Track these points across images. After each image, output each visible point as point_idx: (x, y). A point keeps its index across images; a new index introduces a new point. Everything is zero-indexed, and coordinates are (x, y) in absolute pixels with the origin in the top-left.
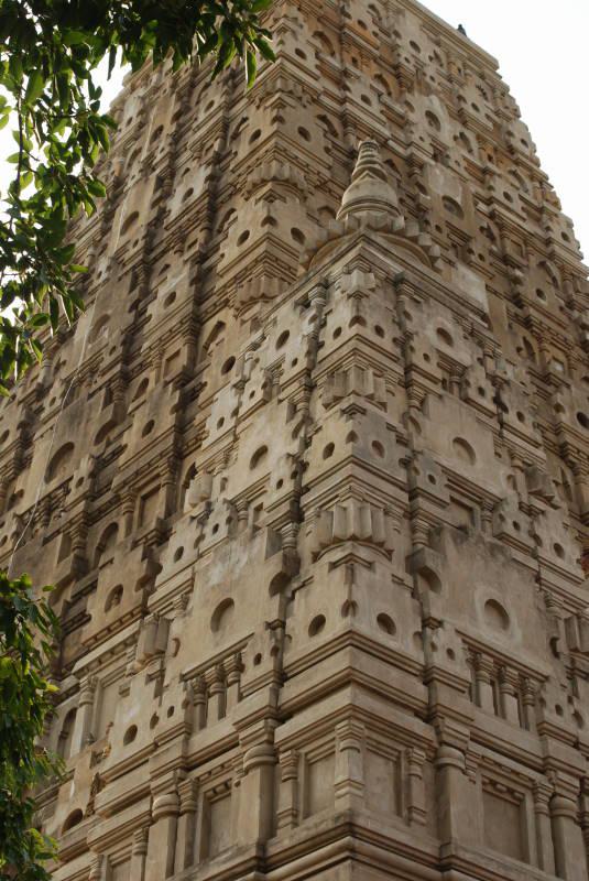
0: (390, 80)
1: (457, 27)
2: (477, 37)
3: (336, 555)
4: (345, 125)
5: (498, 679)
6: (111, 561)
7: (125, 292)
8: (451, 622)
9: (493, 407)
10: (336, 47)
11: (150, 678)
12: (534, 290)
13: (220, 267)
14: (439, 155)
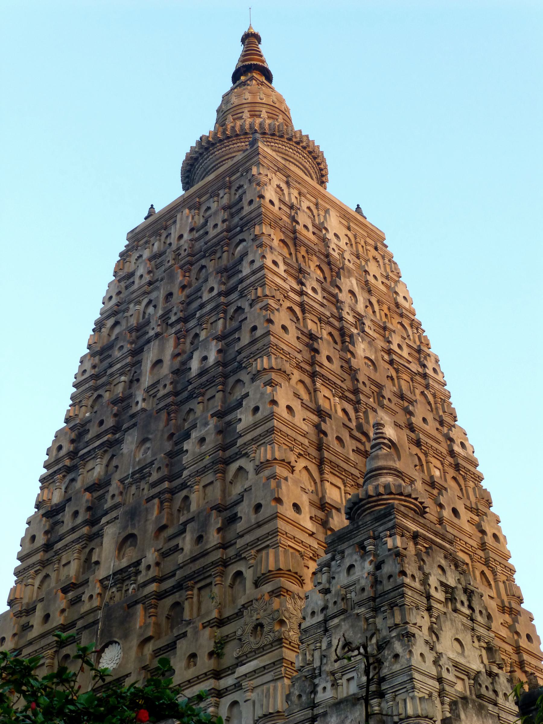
1: (354, 208)
4: (303, 311)
6: (185, 635)
12: (421, 419)
13: (240, 427)
14: (359, 319)
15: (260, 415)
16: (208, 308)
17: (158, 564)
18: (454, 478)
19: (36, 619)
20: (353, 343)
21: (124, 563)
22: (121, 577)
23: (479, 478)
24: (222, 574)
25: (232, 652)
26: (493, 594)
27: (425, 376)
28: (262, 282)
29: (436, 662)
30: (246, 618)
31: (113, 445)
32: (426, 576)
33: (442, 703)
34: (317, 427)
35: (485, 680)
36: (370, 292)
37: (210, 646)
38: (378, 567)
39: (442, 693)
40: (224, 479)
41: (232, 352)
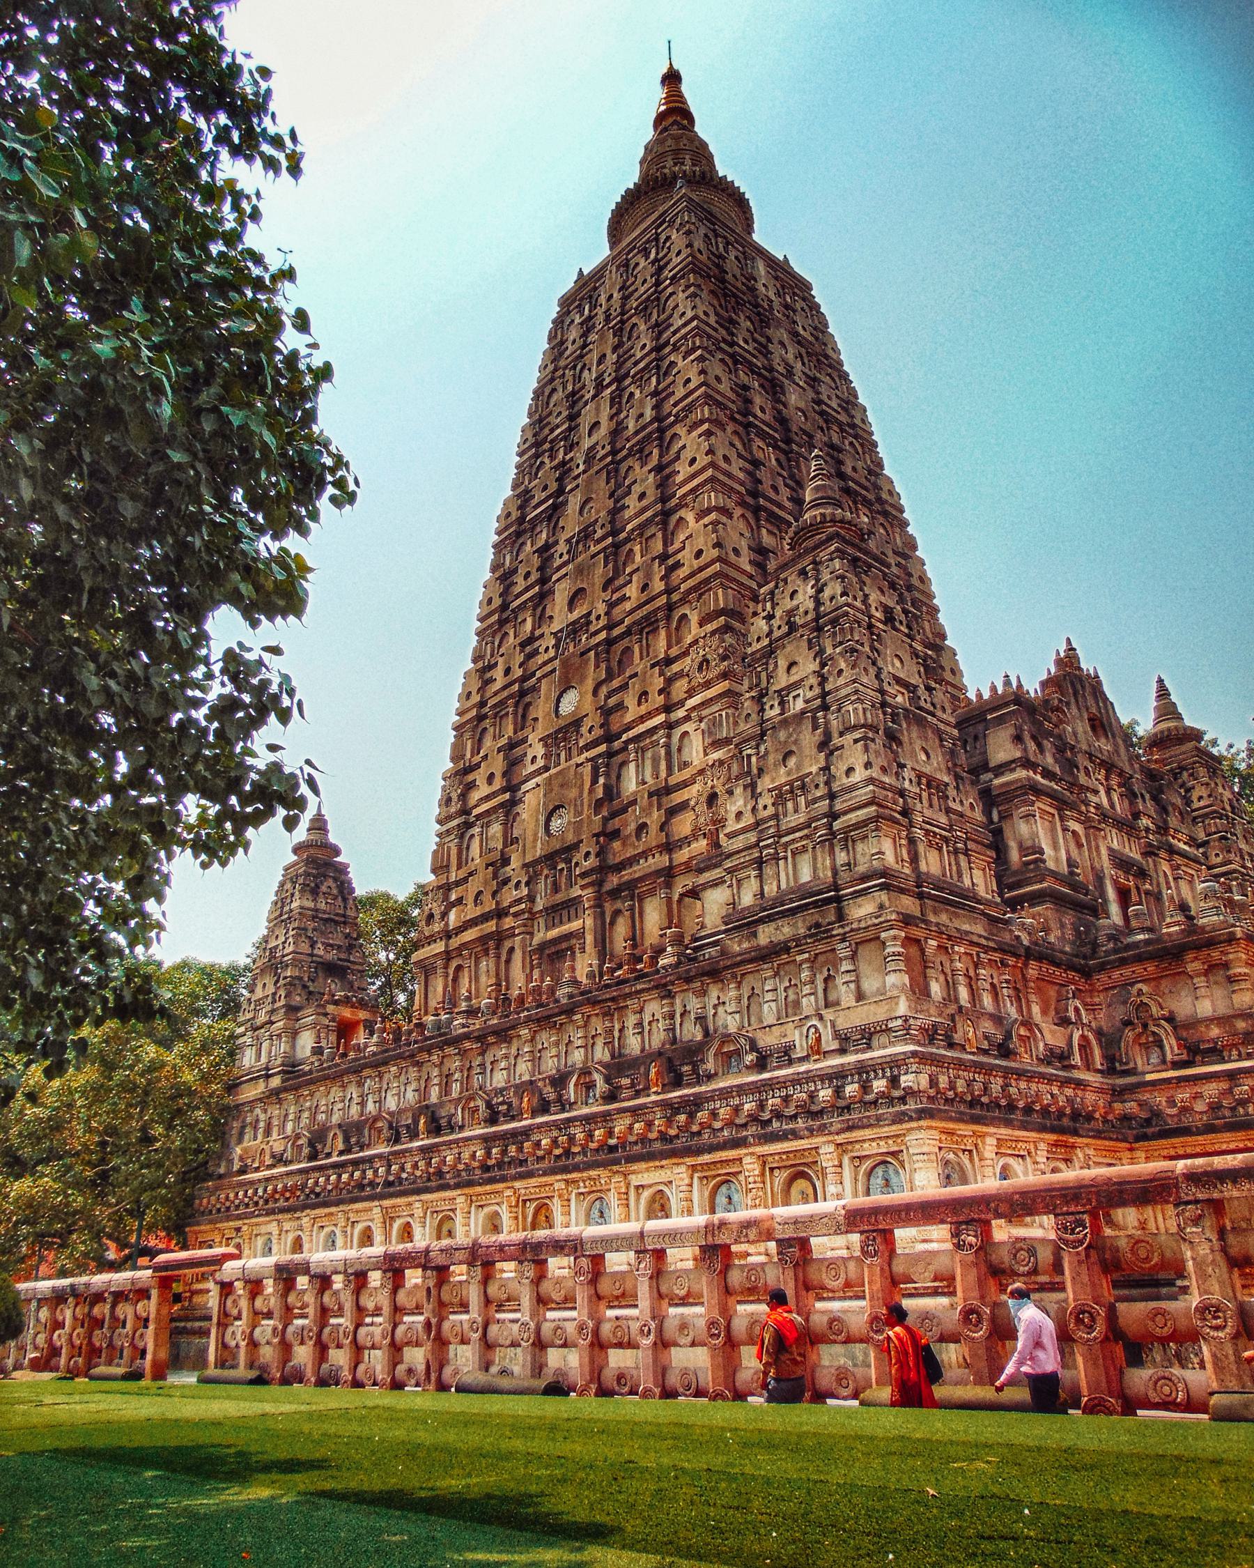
2: (799, 267)
3: (857, 735)
7: (603, 484)
8: (909, 764)
13: (679, 478)
14: (790, 374)
17: (607, 614)
19: (498, 673)
21: (576, 615)
22: (575, 629)
23: (904, 524)
24: (669, 618)
27: (853, 426)
29: (877, 676)
30: (693, 655)
32: (866, 596)
37: (659, 682)
38: (820, 590)
40: (665, 530)
41: (667, 407)
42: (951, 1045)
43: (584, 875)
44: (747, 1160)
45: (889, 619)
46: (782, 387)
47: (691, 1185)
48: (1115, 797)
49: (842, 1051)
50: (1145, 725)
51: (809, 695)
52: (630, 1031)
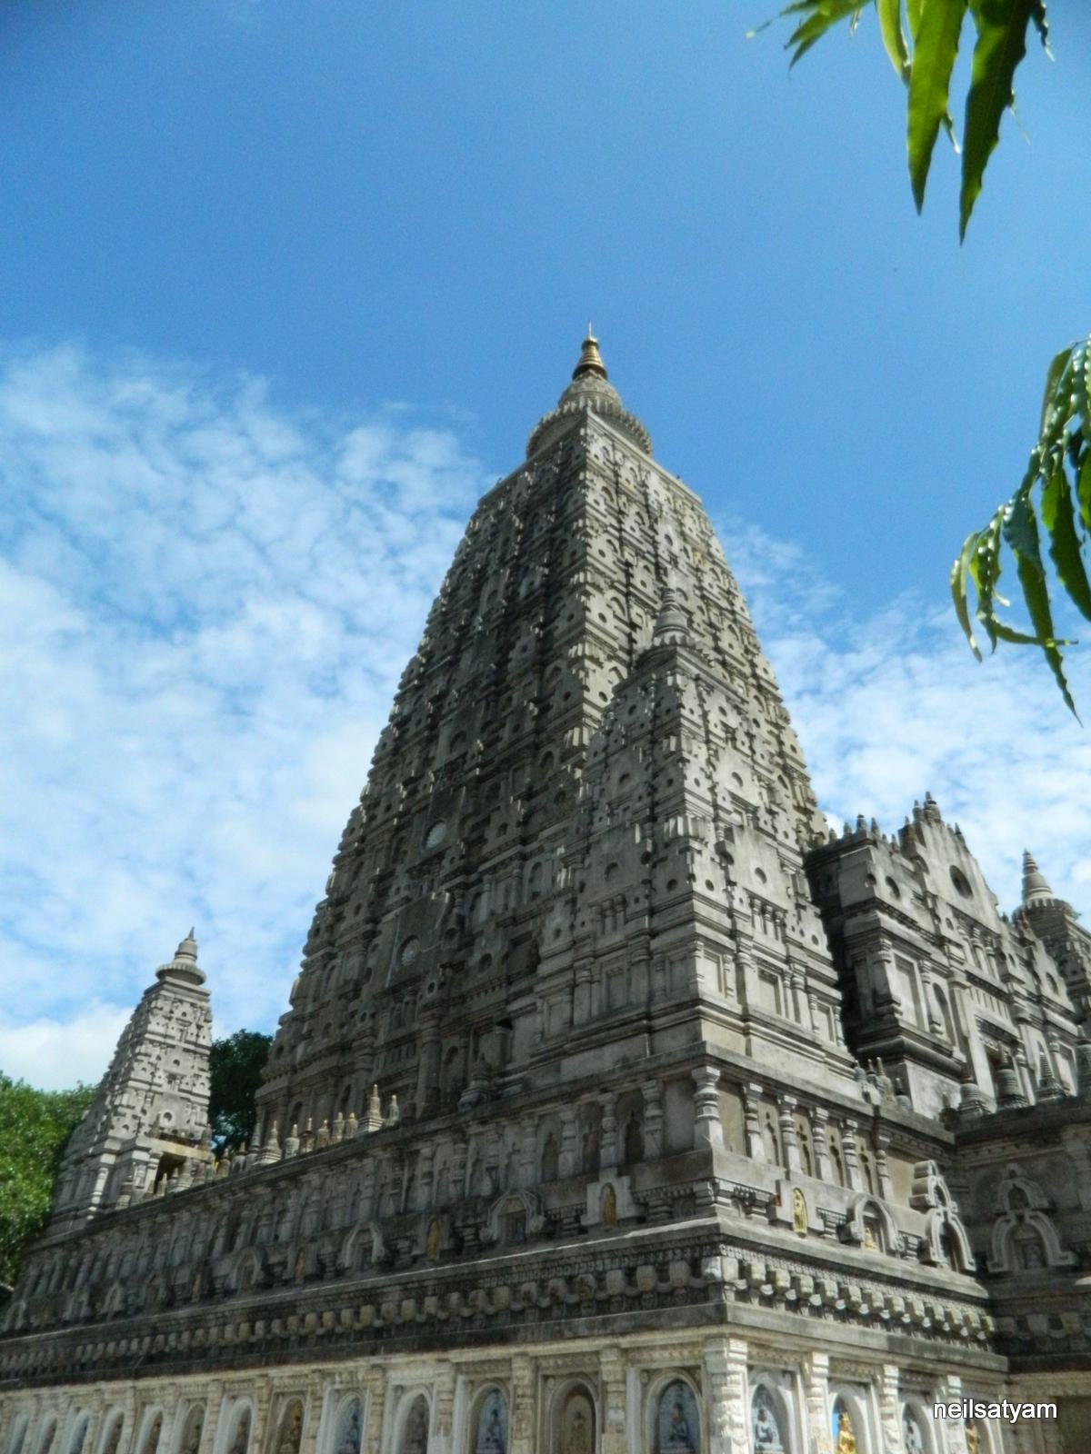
0: (645, 516)
4: (622, 545)
5: (763, 912)
6: (498, 809)
9: (749, 752)
10: (614, 496)
11: (567, 903)
13: (556, 634)
14: (674, 560)
15: (574, 621)
16: (538, 543)
18: (756, 697)
19: (380, 811)
20: (666, 574)
21: (455, 755)
22: (451, 768)
24: (535, 756)
25: (538, 819)
26: (789, 793)
27: (733, 612)
28: (583, 515)
29: (712, 789)
31: (453, 664)
33: (717, 828)
34: (629, 636)
35: (763, 815)
36: (685, 540)
39: (716, 819)
40: (541, 678)
42: (774, 1222)
43: (426, 1007)
44: (518, 1363)
45: (731, 734)
46: (665, 570)
47: (453, 1392)
48: (981, 955)
49: (641, 1221)
50: (1011, 901)
51: (639, 805)
52: (419, 1182)
